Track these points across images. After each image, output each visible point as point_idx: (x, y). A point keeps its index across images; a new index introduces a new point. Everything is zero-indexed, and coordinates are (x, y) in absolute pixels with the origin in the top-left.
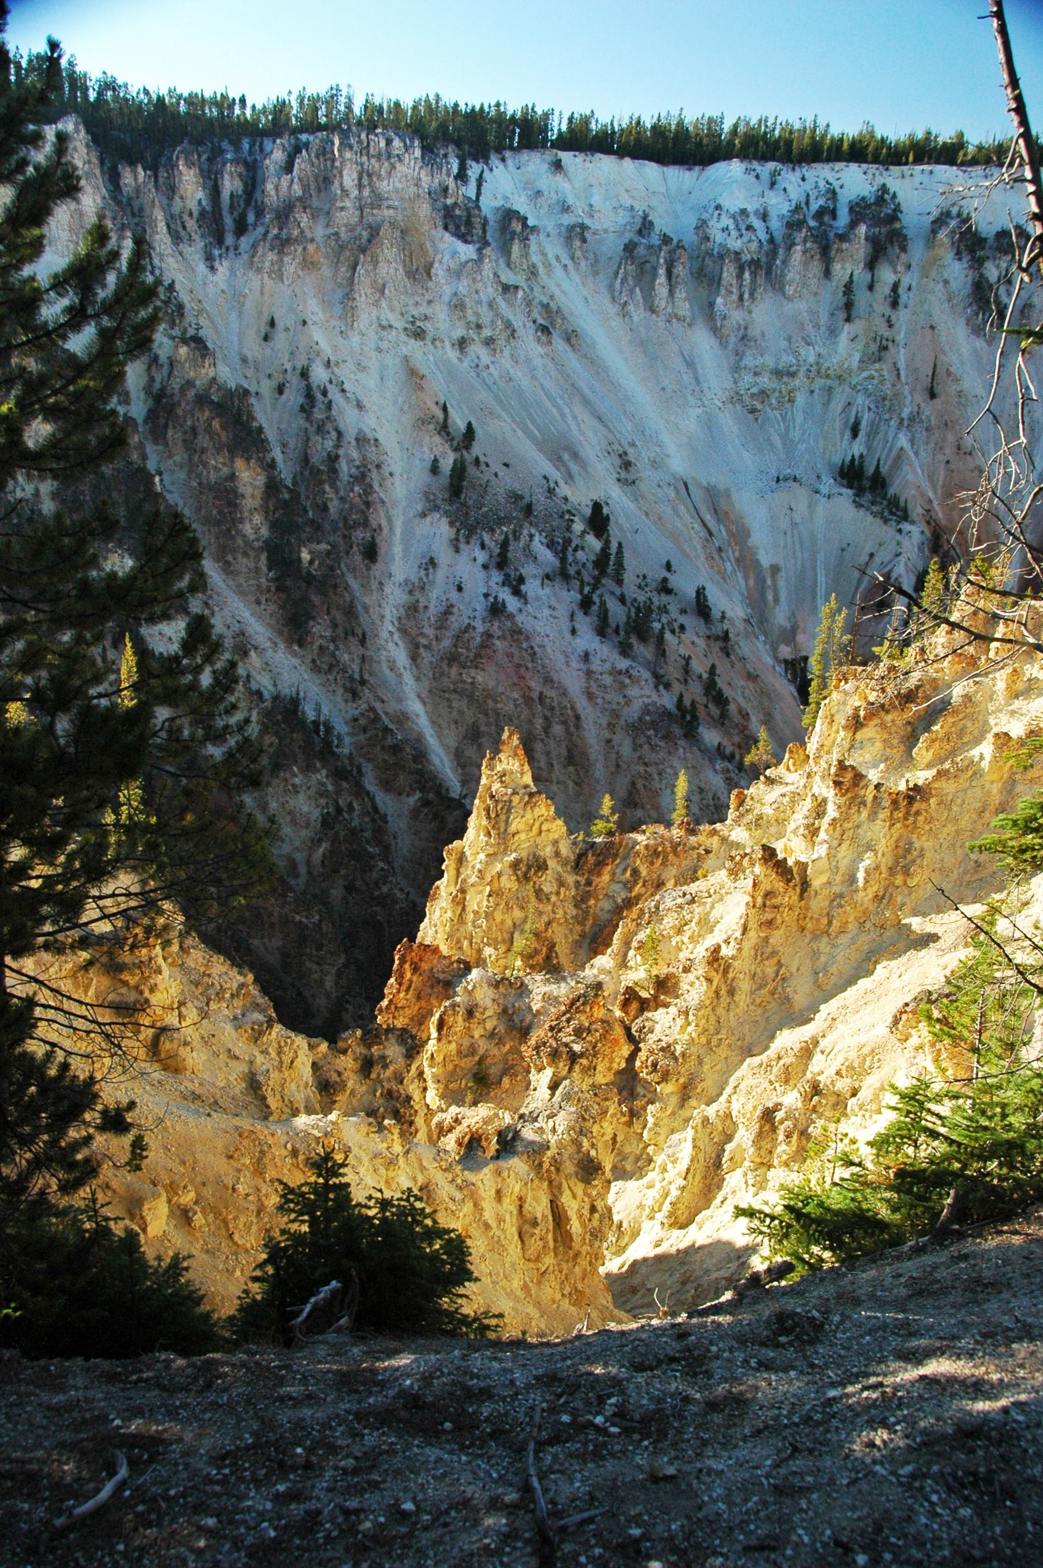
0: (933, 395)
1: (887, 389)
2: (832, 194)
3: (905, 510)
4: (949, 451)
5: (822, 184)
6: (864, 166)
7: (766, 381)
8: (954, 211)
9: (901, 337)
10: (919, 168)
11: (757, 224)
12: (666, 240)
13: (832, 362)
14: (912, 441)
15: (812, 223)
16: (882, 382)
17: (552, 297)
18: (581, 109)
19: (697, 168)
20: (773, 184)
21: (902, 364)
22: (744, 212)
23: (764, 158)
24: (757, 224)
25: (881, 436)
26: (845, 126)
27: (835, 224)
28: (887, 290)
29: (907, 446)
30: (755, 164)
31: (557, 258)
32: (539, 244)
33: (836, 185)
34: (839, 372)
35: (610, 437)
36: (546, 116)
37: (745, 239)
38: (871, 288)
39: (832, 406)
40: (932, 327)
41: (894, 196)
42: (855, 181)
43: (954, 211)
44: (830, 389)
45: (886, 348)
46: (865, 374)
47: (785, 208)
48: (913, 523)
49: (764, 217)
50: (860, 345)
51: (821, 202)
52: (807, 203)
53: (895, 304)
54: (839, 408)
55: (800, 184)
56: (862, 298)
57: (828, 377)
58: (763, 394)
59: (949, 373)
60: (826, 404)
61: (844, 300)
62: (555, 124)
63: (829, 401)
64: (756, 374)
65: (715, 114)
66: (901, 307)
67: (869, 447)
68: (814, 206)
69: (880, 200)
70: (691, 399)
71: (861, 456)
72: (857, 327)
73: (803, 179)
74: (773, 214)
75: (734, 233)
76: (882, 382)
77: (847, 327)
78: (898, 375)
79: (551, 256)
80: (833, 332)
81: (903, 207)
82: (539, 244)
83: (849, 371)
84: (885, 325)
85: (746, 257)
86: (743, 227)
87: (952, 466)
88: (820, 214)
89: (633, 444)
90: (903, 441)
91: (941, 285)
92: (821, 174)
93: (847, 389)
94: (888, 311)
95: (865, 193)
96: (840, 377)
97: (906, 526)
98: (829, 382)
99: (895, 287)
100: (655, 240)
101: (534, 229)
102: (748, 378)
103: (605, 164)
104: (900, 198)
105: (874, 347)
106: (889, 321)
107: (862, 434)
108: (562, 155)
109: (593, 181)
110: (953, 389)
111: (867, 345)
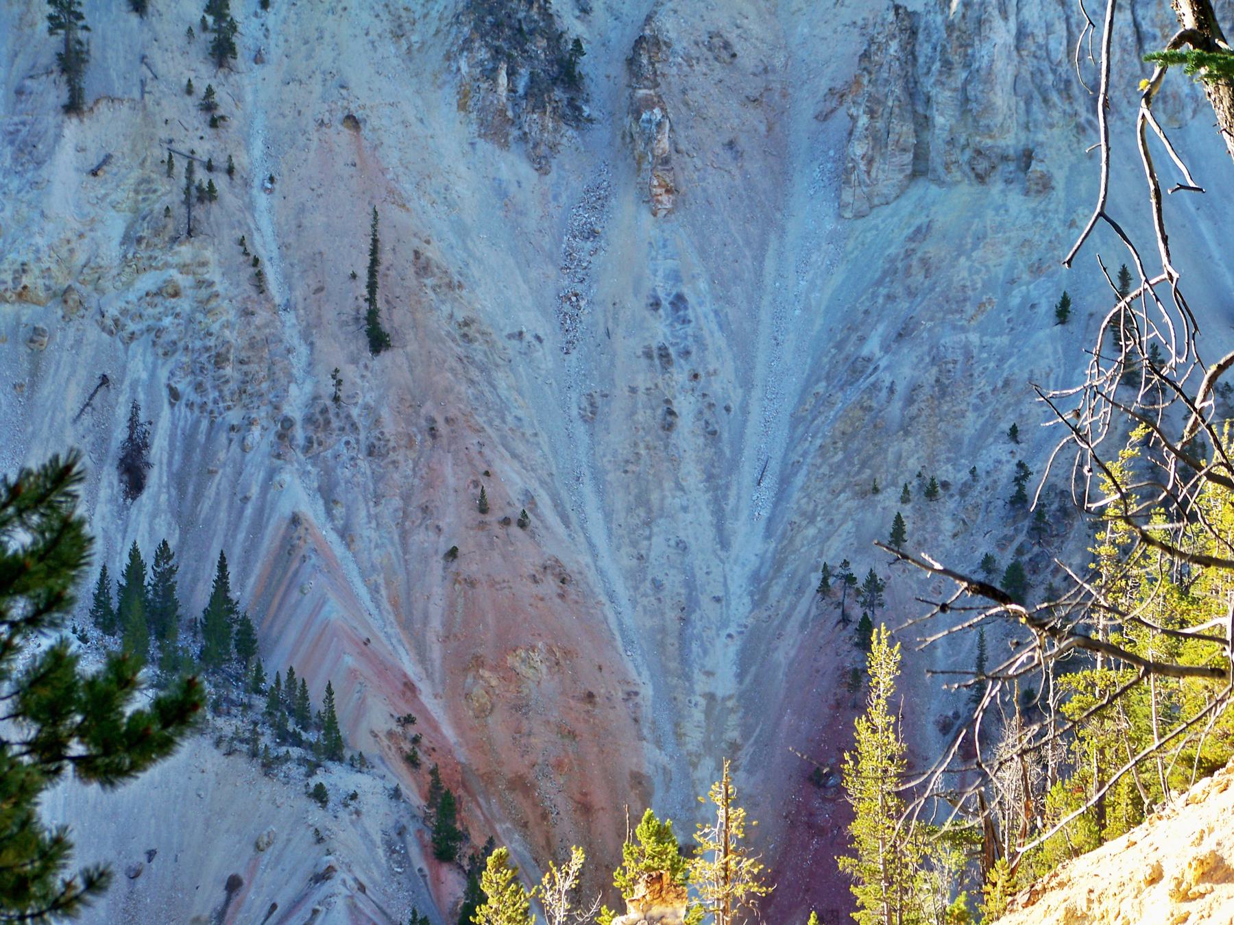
0: (378, 341)
1: (225, 325)
3: (329, 724)
9: (252, 158)
16: (204, 305)
21: (265, 245)
25: (219, 482)
29: (312, 510)
34: (62, 282)
39: (46, 390)
40: (352, 121)
44: (35, 335)
45: (208, 194)
46: (148, 282)
48: (360, 763)
50: (120, 189)
54: (73, 399)
57: (23, 295)
59: (423, 267)
61: (56, 42)
63: (35, 374)
66: (242, 61)
67: (185, 518)
71: (164, 552)
72: (104, 128)
76: (204, 305)
77: (72, 128)
78: (259, 280)
80: (29, 151)
83: (94, 272)
84: (197, 120)
87: (469, 566)
90: (297, 493)
93: (93, 333)
94: (204, 75)
96: (63, 295)
97: (337, 778)
98: (28, 313)
105: (169, 193)
106: (208, 106)
107: (156, 478)
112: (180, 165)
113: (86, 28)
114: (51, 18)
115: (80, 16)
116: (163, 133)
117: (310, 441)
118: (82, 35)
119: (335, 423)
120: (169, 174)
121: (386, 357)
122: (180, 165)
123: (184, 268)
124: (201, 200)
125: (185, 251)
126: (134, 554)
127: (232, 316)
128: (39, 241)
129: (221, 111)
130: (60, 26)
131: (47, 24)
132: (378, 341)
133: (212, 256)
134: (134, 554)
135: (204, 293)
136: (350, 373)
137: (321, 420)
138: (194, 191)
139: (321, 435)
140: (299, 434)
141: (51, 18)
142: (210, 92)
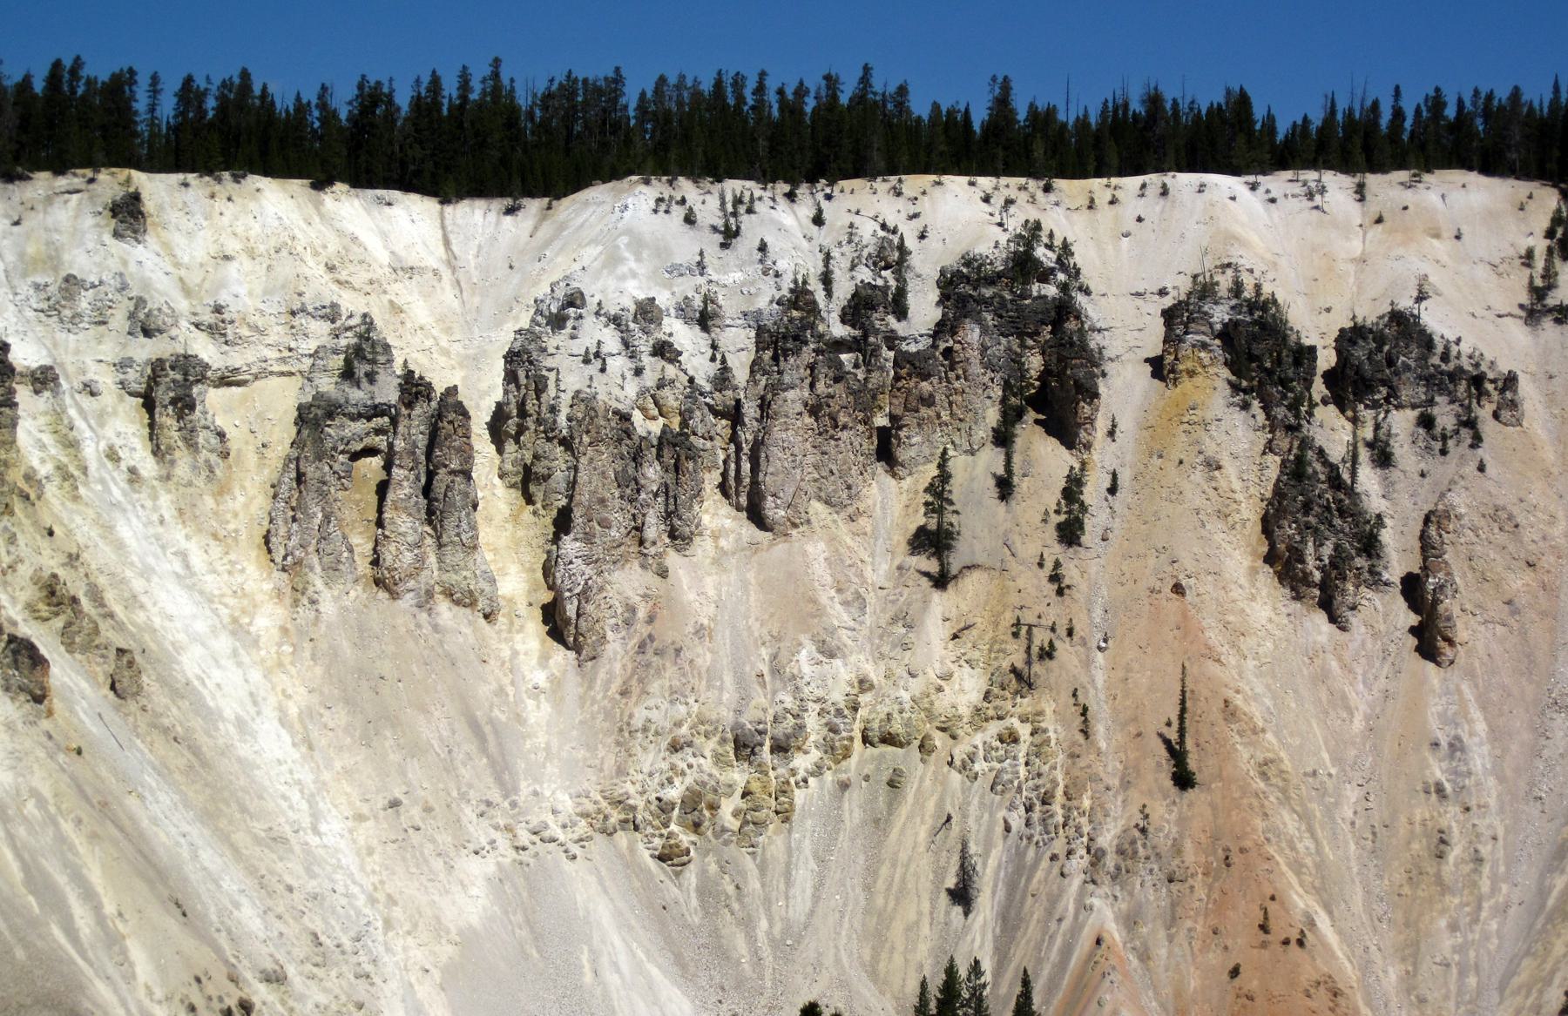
0: (1183, 780)
2: (892, 256)
4: (1242, 941)
5: (868, 231)
6: (986, 182)
7: (703, 764)
8: (1225, 281)
10: (1132, 183)
11: (684, 336)
12: (414, 388)
13: (894, 700)
14: (1131, 921)
15: (839, 330)
16: (1039, 750)
17: (73, 559)
18: (214, 72)
19: (533, 206)
20: (729, 235)
22: (647, 312)
23: (712, 169)
24: (684, 336)
26: (945, 86)
27: (900, 328)
28: (1052, 497)
29: (1115, 933)
30: (686, 187)
31: (113, 456)
32: (58, 414)
33: (909, 232)
35: (203, 958)
36: (120, 86)
37: (650, 378)
38: (1005, 487)
40: (1178, 589)
41: (1066, 248)
42: (959, 216)
43: (1225, 281)
45: (1047, 653)
47: (765, 298)
49: (705, 320)
51: (865, 274)
52: (827, 280)
53: (1070, 533)
55: (798, 235)
56: (978, 522)
58: (697, 808)
60: (878, 824)
62: (141, 104)
64: (675, 747)
65: (594, 70)
68: (844, 289)
69: (1023, 265)
70: (481, 833)
73: (818, 220)
74: (729, 306)
75: (618, 364)
77: (940, 603)
79: (91, 451)
81: (1089, 277)
82: (58, 414)
85: (647, 426)
86: (644, 345)
87: (1250, 981)
88: (860, 307)
89: (275, 978)
90: (1105, 914)
91: (1198, 476)
92: (867, 206)
94: (1055, 550)
95: (983, 249)
99: (1072, 490)
100: (388, 391)
101: (44, 379)
102: (651, 759)
103: (274, 203)
104: (1079, 258)
106: (1055, 578)
108: (141, 179)
109: (232, 246)
110: (1245, 757)
111: (995, 648)
112: (1024, 630)
113: (957, 512)
114: (927, 504)
115: (951, 503)
116: (1014, 599)
117: (1118, 868)
118: (954, 519)
119: (1141, 852)
120: (1016, 635)
121: (1191, 794)
122: (1024, 630)
123: (1024, 720)
124: (1041, 657)
125: (1026, 704)
126: (951, 971)
127: (1061, 758)
128: (906, 696)
129: (1067, 581)
130: (933, 511)
131: (923, 510)
132: (1183, 780)
133: (1050, 707)
134: (951, 971)
135: (1038, 739)
136: (1158, 810)
137: (1130, 851)
138: (1035, 650)
139: (1129, 862)
140: (1110, 861)
141: (927, 504)
142: (1057, 564)
